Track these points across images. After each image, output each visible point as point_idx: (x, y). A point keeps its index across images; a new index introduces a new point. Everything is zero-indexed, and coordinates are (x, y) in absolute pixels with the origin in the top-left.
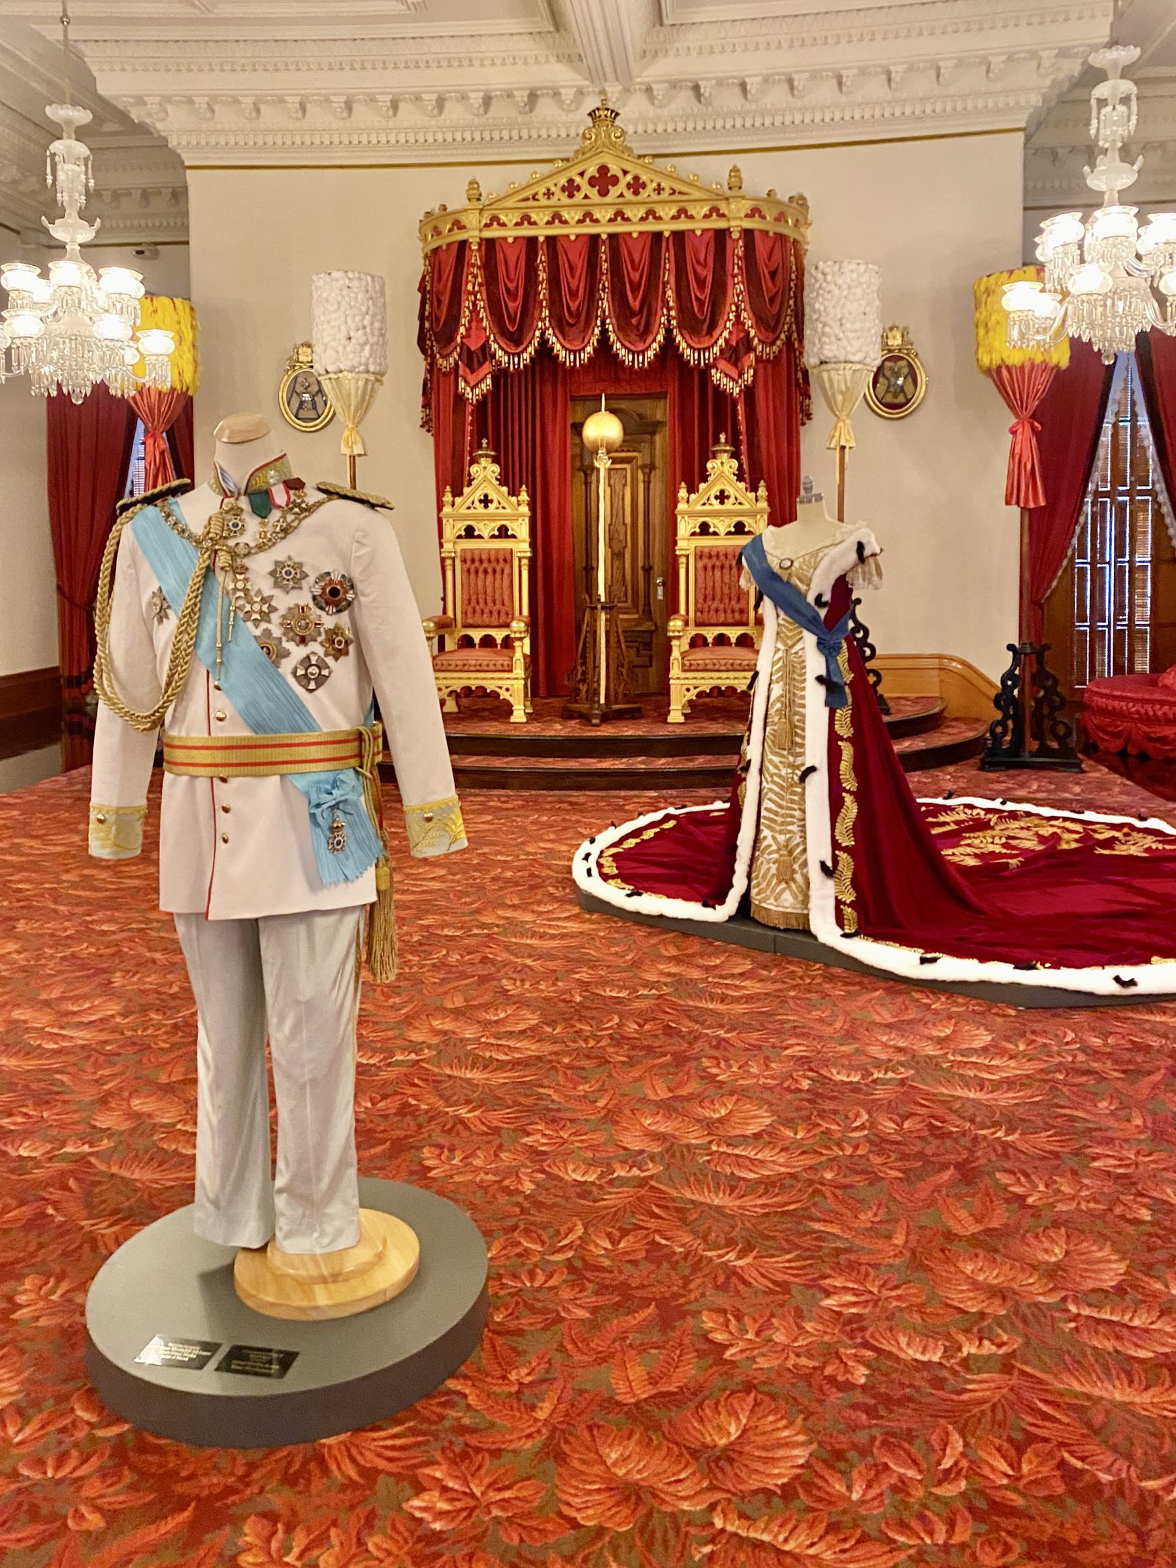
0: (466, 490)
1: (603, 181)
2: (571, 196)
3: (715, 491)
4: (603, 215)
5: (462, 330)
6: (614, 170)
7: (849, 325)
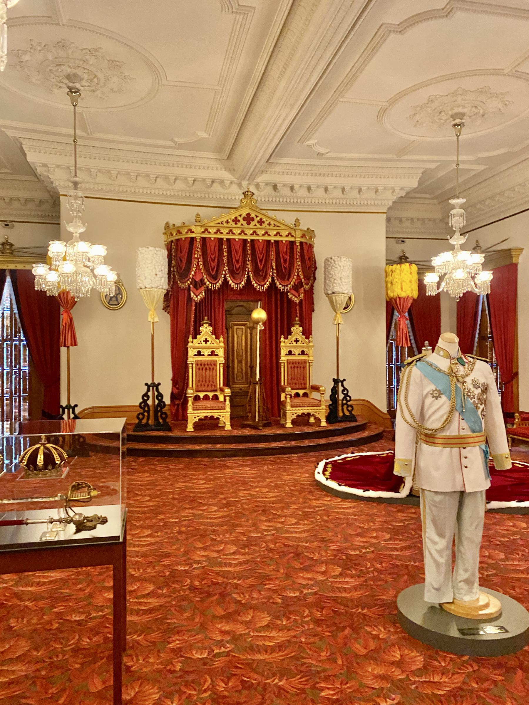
0: (198, 336)
1: (248, 219)
2: (236, 224)
3: (294, 339)
4: (249, 232)
5: (193, 273)
6: (253, 215)
7: (343, 280)
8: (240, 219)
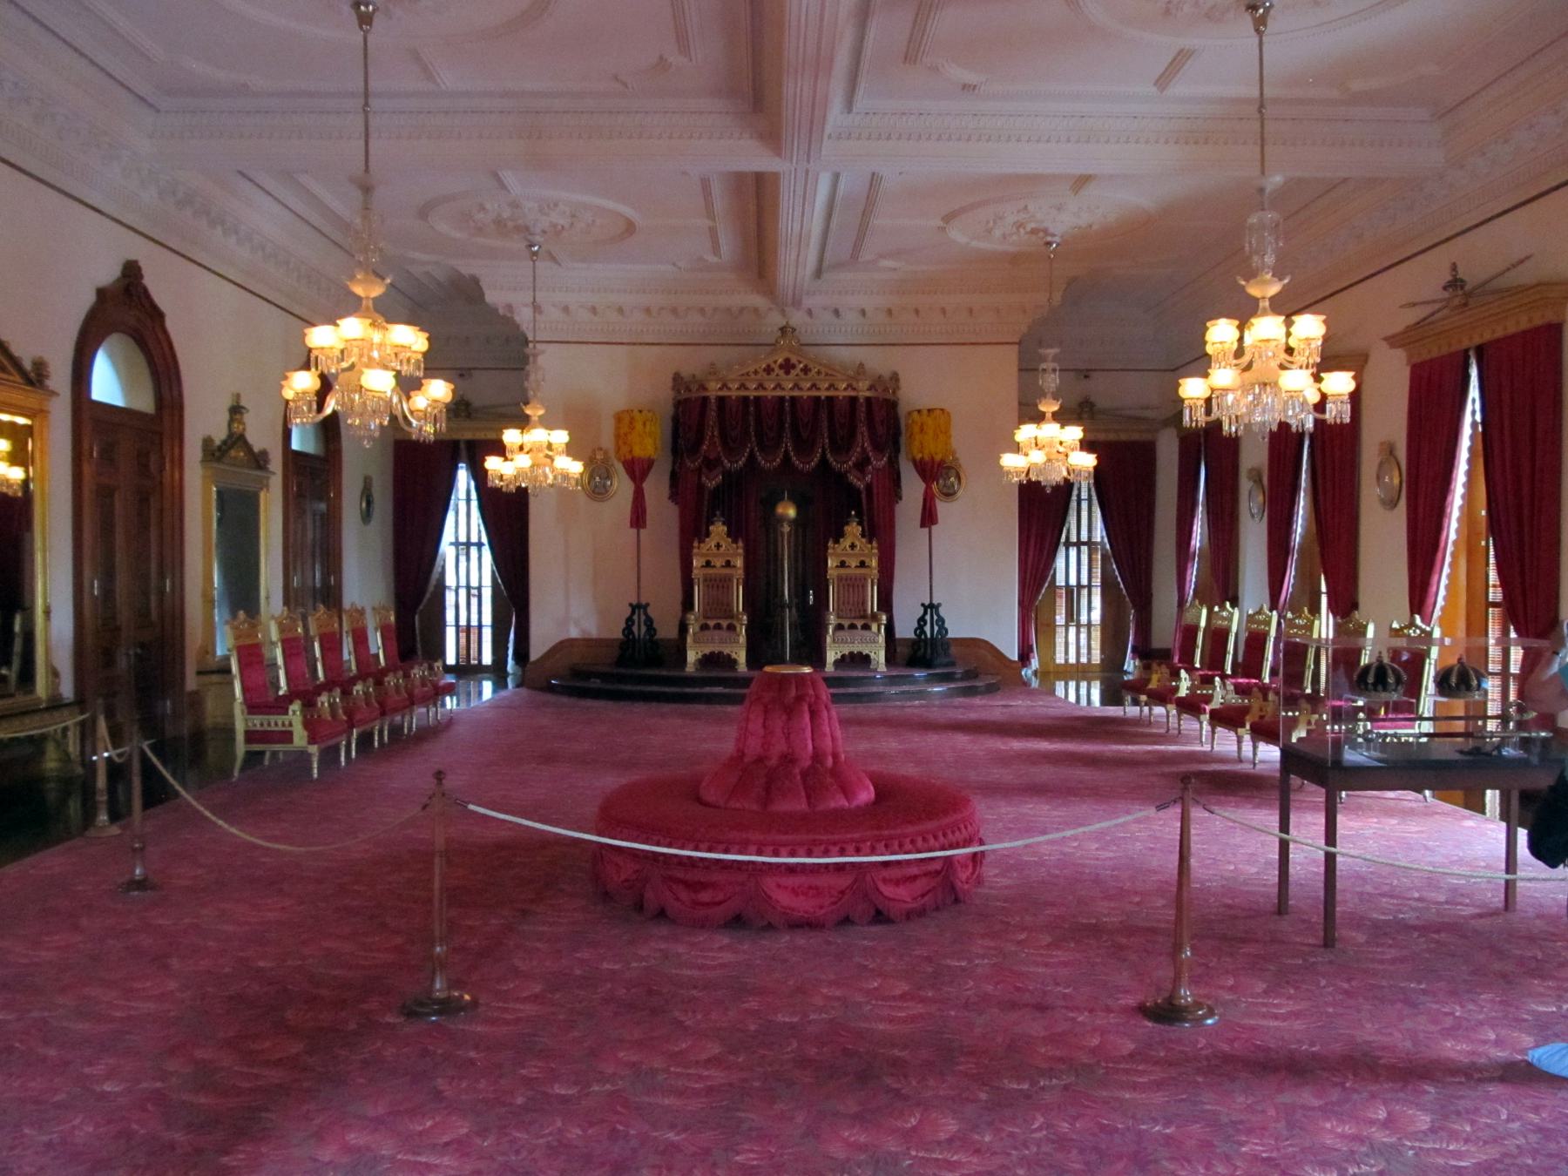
1: (787, 366)
6: (794, 360)
8: (776, 368)
